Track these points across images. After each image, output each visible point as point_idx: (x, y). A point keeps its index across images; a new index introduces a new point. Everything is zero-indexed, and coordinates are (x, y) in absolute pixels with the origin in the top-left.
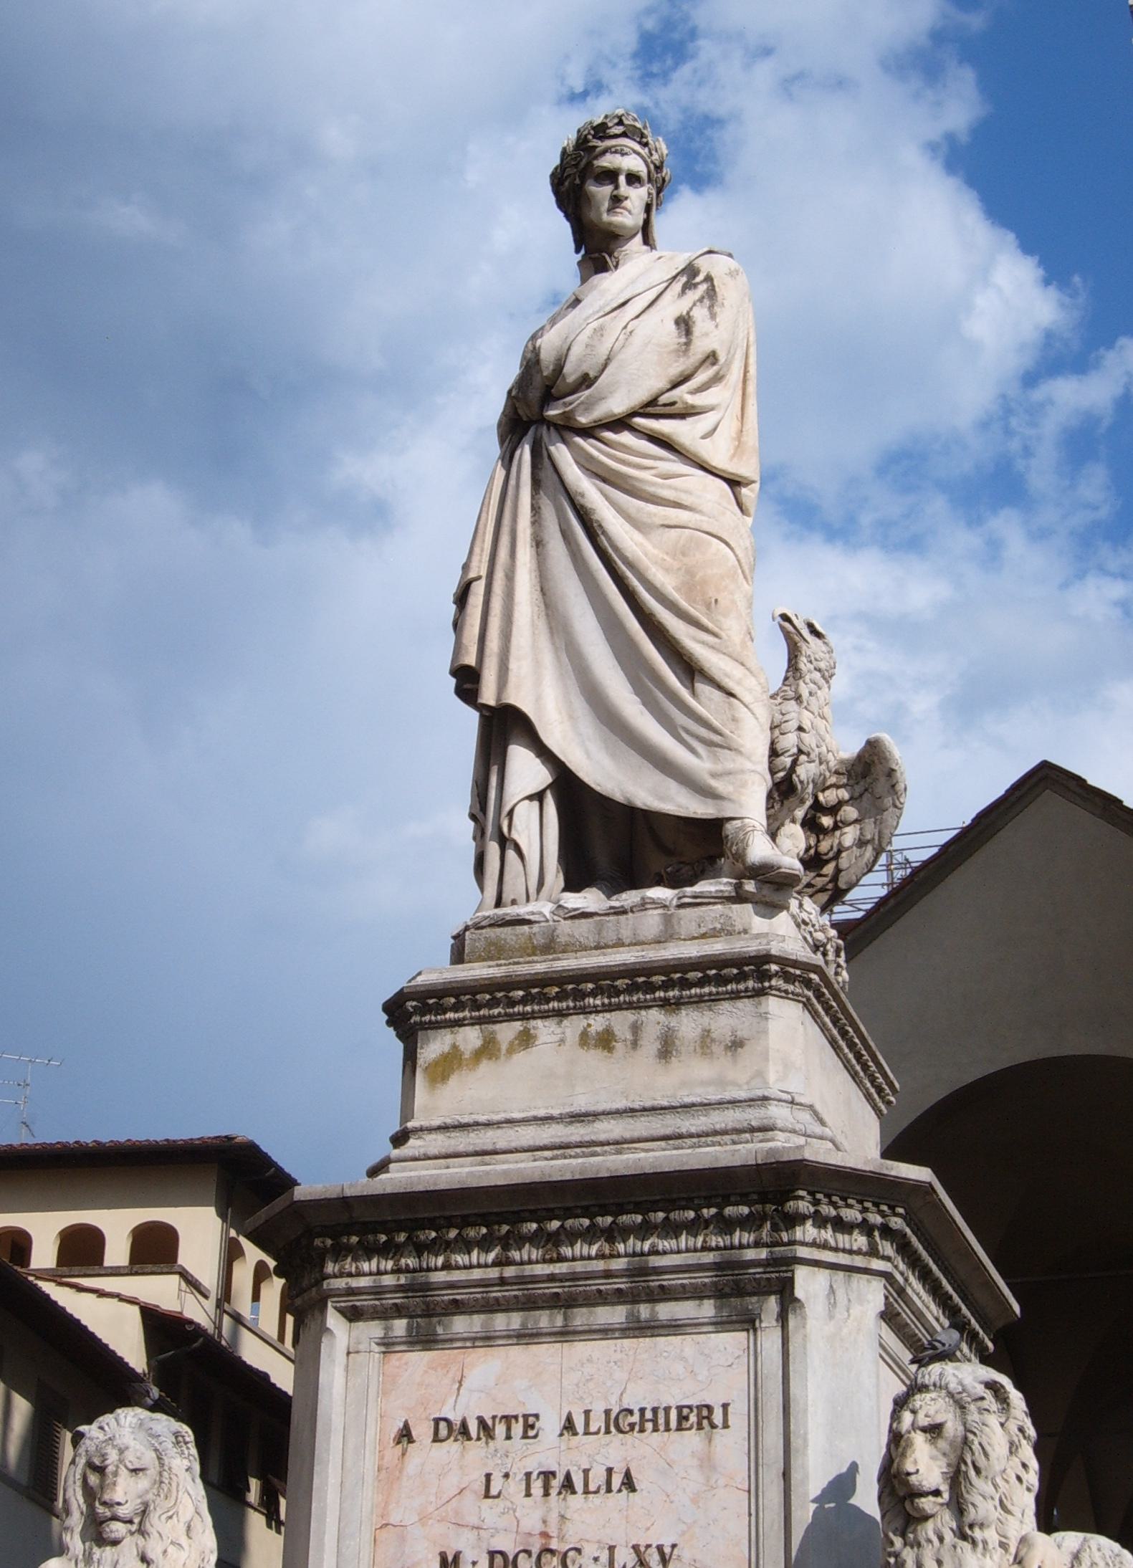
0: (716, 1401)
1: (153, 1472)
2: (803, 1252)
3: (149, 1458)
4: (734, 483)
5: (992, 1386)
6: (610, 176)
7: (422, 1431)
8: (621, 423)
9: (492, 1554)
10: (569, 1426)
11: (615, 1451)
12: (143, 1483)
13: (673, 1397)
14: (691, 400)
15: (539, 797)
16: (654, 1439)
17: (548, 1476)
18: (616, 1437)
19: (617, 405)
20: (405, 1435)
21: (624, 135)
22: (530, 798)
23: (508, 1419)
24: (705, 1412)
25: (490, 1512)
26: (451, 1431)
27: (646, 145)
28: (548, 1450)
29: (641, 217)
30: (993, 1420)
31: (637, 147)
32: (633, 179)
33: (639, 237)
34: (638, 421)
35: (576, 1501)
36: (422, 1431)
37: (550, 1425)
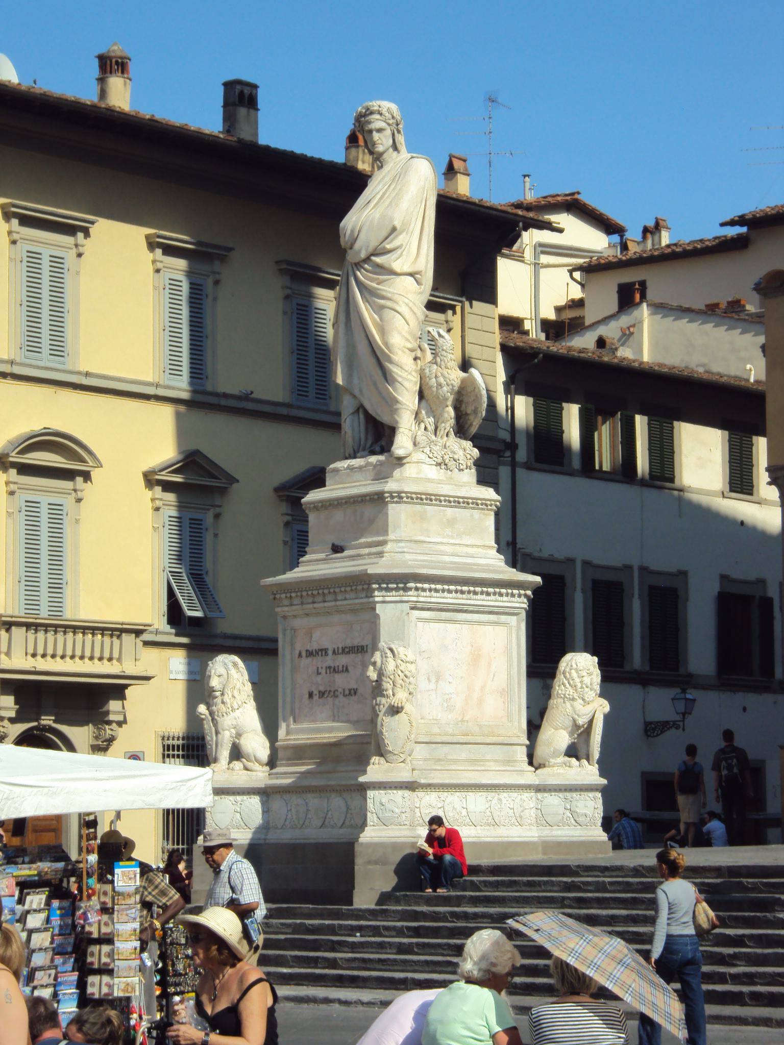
0: (364, 643)
1: (226, 676)
2: (377, 599)
3: (222, 671)
4: (411, 275)
5: (391, 650)
6: (371, 131)
7: (304, 654)
8: (367, 259)
9: (320, 692)
10: (334, 652)
11: (343, 660)
12: (222, 679)
13: (357, 642)
14: (388, 247)
15: (357, 411)
16: (352, 656)
17: (330, 667)
18: (344, 655)
19: (363, 255)
20: (300, 655)
21: (372, 113)
22: (353, 413)
23: (321, 650)
24: (362, 647)
25: (319, 679)
26: (310, 654)
27: (381, 114)
28: (329, 661)
29: (391, 141)
30: (391, 660)
31: (378, 117)
32: (379, 130)
33: (391, 150)
34: (373, 258)
35: (337, 676)
36: (304, 654)
37: (330, 652)
